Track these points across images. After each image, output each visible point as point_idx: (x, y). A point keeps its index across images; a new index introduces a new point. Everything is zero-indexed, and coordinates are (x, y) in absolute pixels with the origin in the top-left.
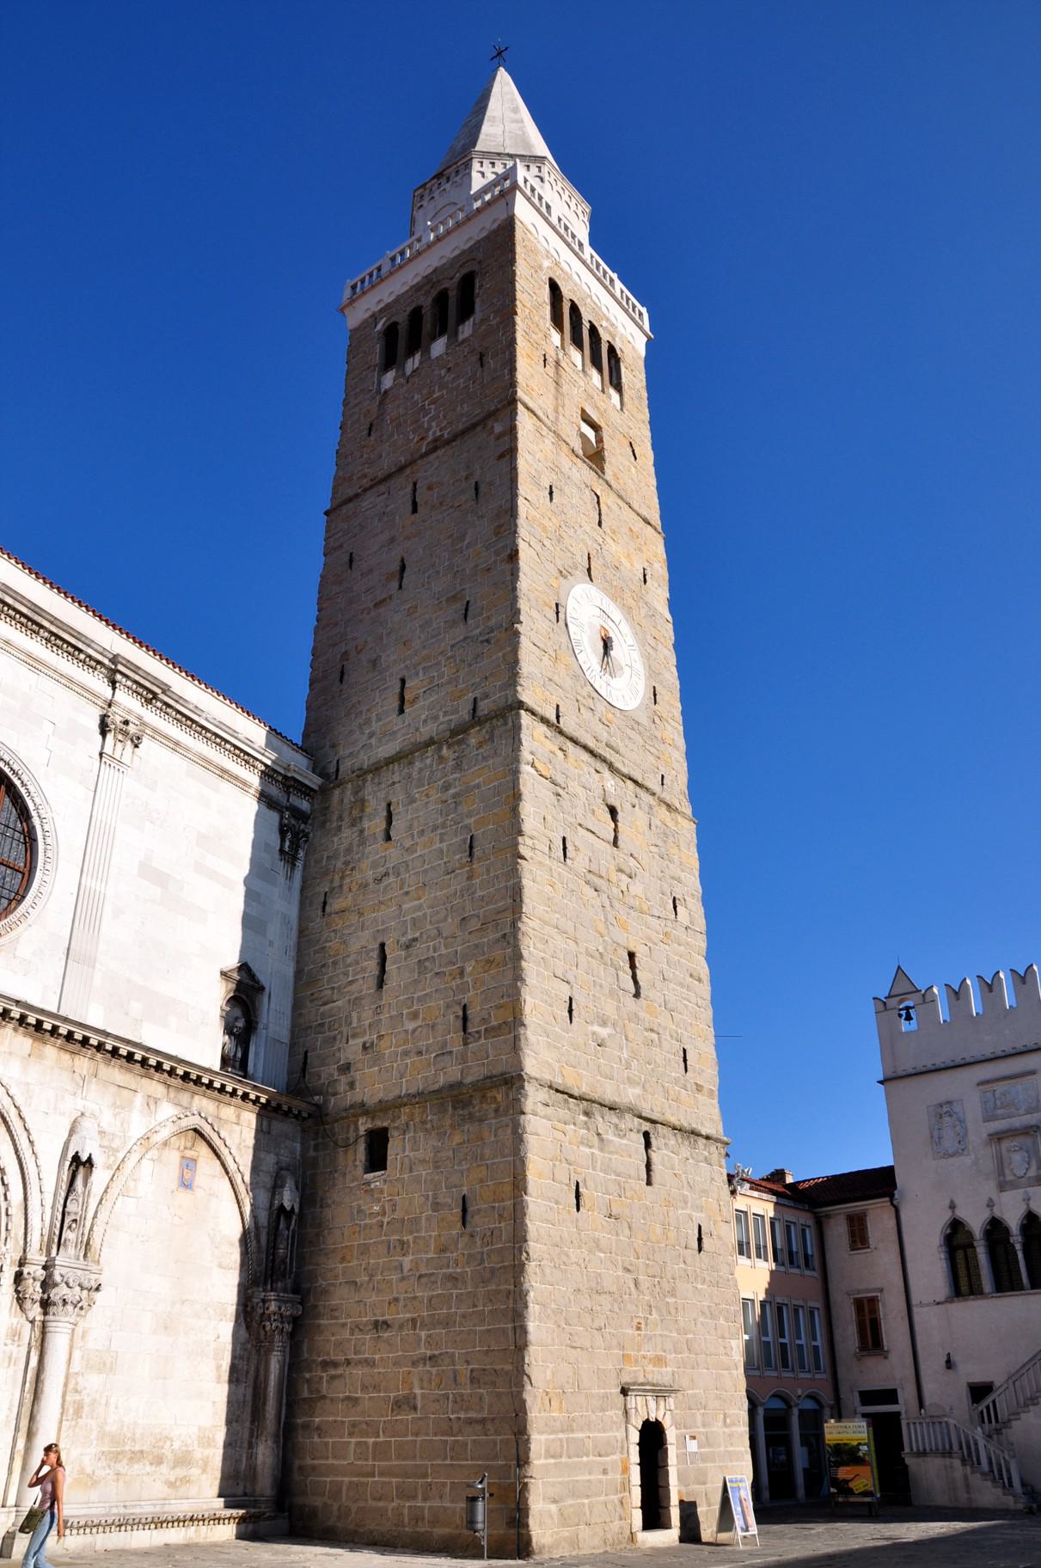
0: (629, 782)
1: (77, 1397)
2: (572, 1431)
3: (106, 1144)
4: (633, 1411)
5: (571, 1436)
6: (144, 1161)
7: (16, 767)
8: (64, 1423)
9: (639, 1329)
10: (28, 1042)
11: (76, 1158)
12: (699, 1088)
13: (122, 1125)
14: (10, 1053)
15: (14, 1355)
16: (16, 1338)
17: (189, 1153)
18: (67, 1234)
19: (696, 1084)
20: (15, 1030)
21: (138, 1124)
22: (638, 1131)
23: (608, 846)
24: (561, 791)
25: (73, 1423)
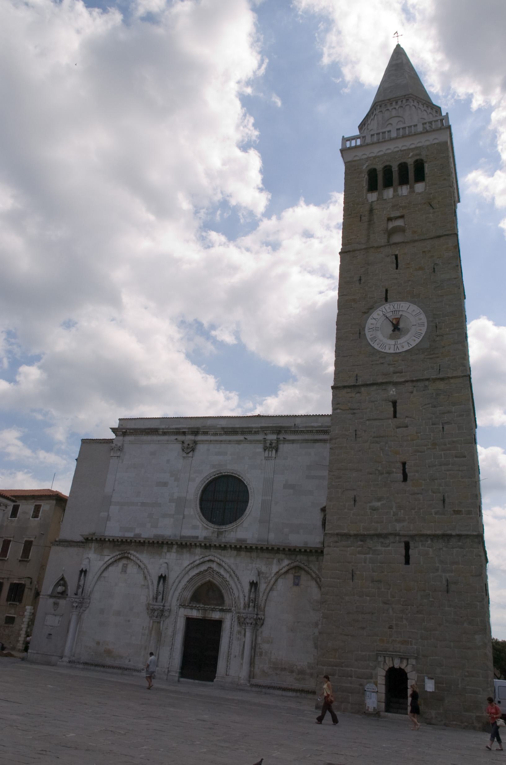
0: (407, 384)
1: (260, 650)
2: (342, 667)
3: (264, 576)
4: (382, 663)
5: (341, 668)
6: (279, 580)
7: (238, 474)
8: (256, 658)
9: (391, 627)
10: (235, 553)
11: (250, 582)
12: (458, 512)
13: (269, 569)
14: (230, 556)
15: (240, 638)
16: (240, 633)
17: (296, 574)
18: (251, 604)
19: (454, 511)
20: (231, 550)
21: (275, 569)
22: (400, 542)
23: (390, 421)
24: (355, 411)
25: (260, 658)
